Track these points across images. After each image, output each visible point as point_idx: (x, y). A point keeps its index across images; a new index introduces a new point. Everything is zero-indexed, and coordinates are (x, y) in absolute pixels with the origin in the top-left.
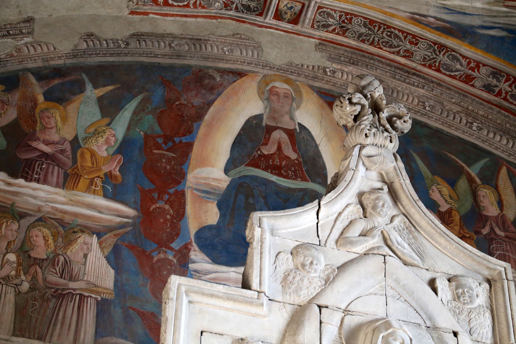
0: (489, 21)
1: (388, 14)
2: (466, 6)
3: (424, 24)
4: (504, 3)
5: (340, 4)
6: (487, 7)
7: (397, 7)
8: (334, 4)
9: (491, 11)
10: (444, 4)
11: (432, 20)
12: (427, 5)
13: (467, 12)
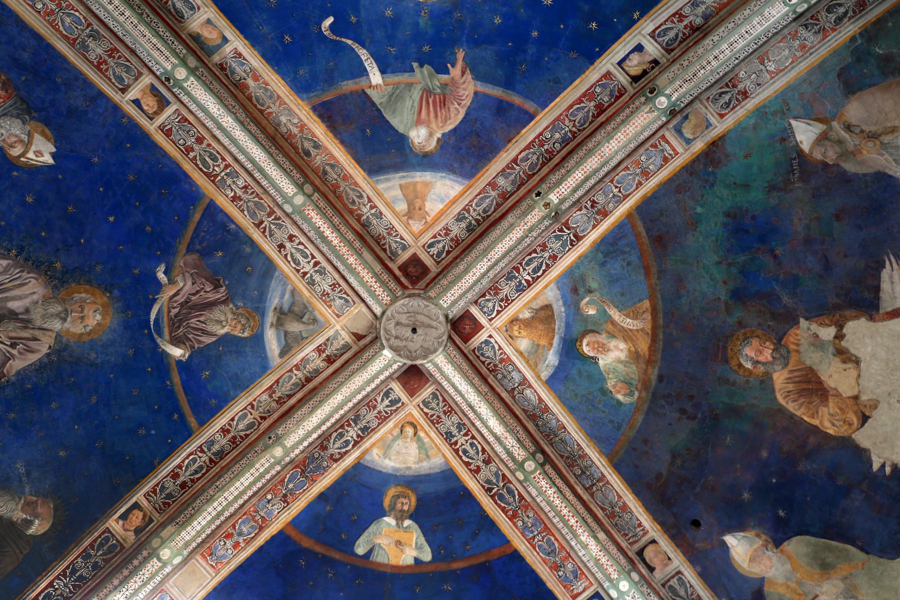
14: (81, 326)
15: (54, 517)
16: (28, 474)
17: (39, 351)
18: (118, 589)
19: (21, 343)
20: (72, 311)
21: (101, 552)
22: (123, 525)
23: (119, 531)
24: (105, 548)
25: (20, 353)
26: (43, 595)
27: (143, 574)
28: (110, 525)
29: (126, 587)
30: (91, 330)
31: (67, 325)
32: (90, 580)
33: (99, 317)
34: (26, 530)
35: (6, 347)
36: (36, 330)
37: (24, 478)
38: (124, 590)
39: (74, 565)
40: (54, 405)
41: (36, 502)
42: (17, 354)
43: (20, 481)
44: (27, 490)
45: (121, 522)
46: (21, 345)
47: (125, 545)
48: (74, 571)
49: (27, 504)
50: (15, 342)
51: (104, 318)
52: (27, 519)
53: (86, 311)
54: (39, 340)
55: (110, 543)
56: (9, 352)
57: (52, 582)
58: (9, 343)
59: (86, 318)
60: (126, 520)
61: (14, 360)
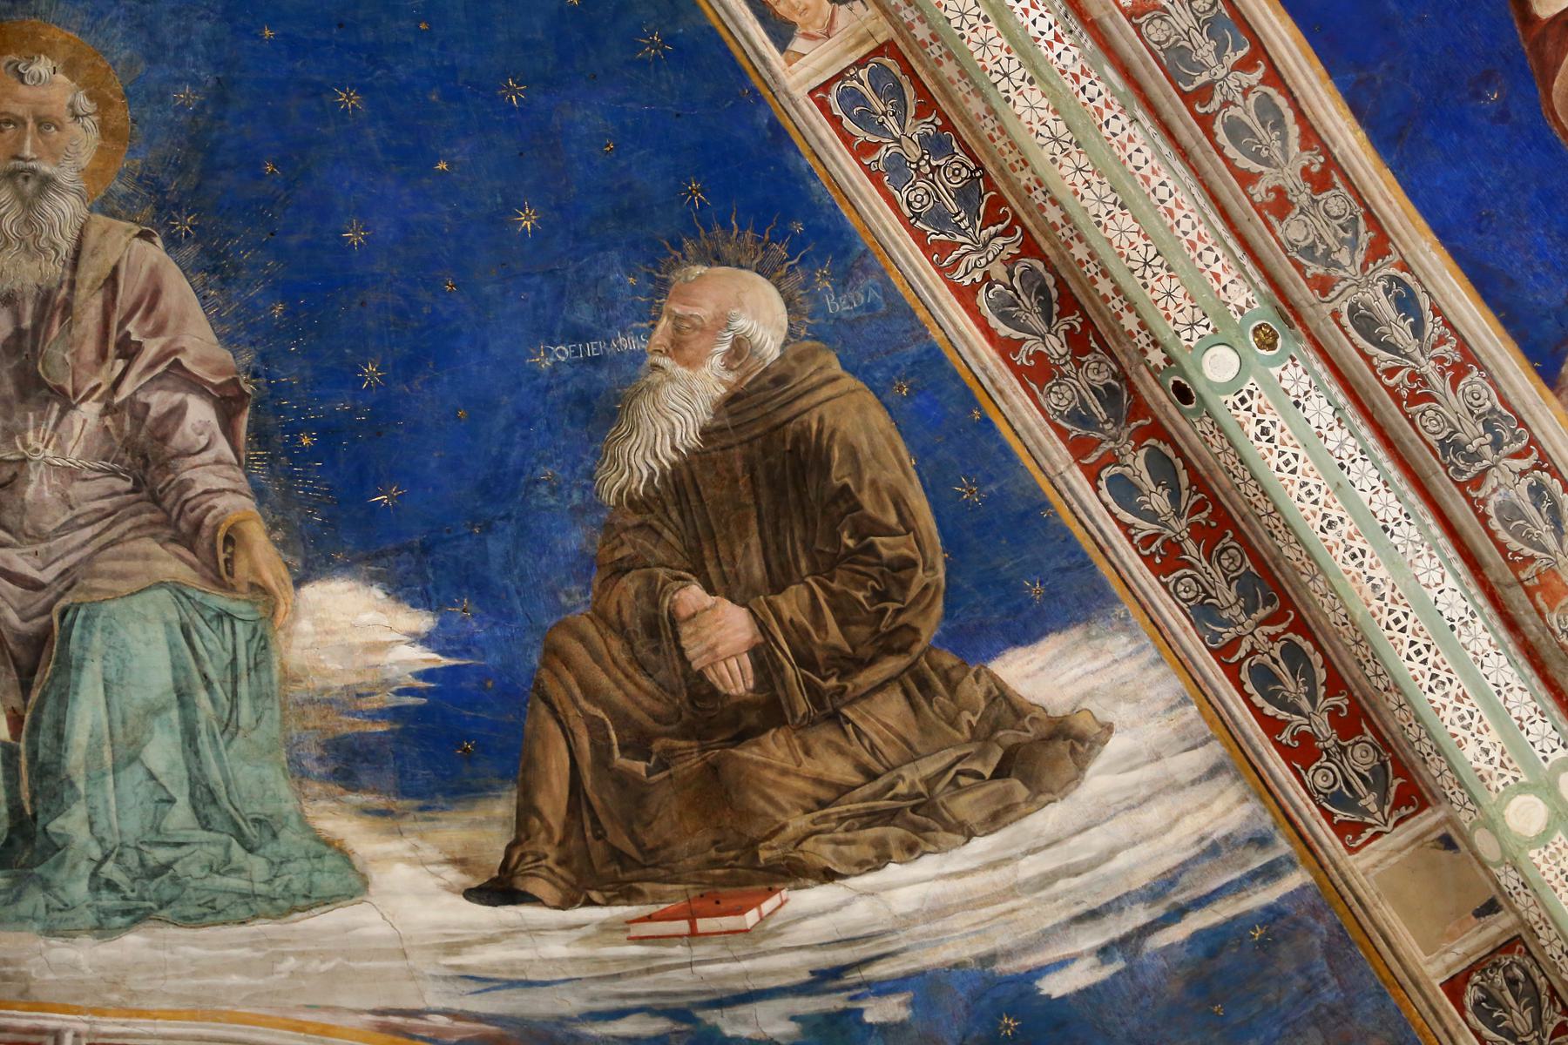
0: (605, 995)
1: (309, 1028)
2: (523, 961)
3: (423, 1039)
4: (627, 930)
5: (155, 1025)
6: (582, 951)
7: (331, 1003)
8: (137, 1030)
9: (601, 961)
10: (459, 967)
11: (441, 1021)
12: (413, 979)
13: (531, 977)
14: (75, 128)
15: (741, 267)
16: (577, 335)
17: (154, 273)
18: (997, 104)
19: (122, 325)
20: (16, 157)
21: (891, 123)
22: (808, 36)
23: (825, 57)
24: (878, 106)
25: (158, 331)
26: (994, 322)
27: (963, 15)
28: (800, 83)
29: (995, 78)
30: (90, 97)
31: (66, 175)
32: (980, 167)
33: (43, 67)
34: (763, 360)
35: (132, 374)
36: (80, 275)
37: (591, 349)
38: (1002, 86)
39: (917, 216)
40: (354, 237)
41: (679, 318)
42: (162, 340)
43: (596, 362)
44: (628, 343)
45: (798, 45)
46: (130, 327)
47: (881, 39)
48: (940, 218)
49: (676, 347)
50: (118, 346)
51: (48, 49)
52: (728, 353)
53: (18, 110)
54: (115, 269)
55: (866, 90)
56: (152, 366)
57: (957, 290)
58: (120, 365)
59: (44, 111)
60: (793, 25)
61: (183, 350)
